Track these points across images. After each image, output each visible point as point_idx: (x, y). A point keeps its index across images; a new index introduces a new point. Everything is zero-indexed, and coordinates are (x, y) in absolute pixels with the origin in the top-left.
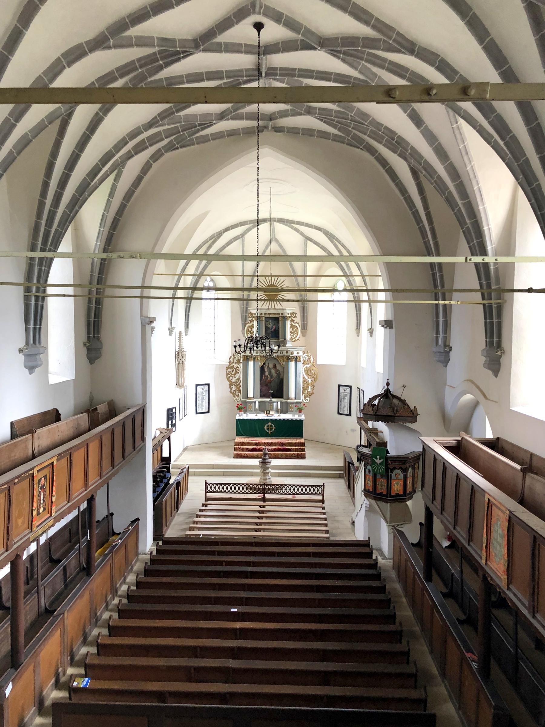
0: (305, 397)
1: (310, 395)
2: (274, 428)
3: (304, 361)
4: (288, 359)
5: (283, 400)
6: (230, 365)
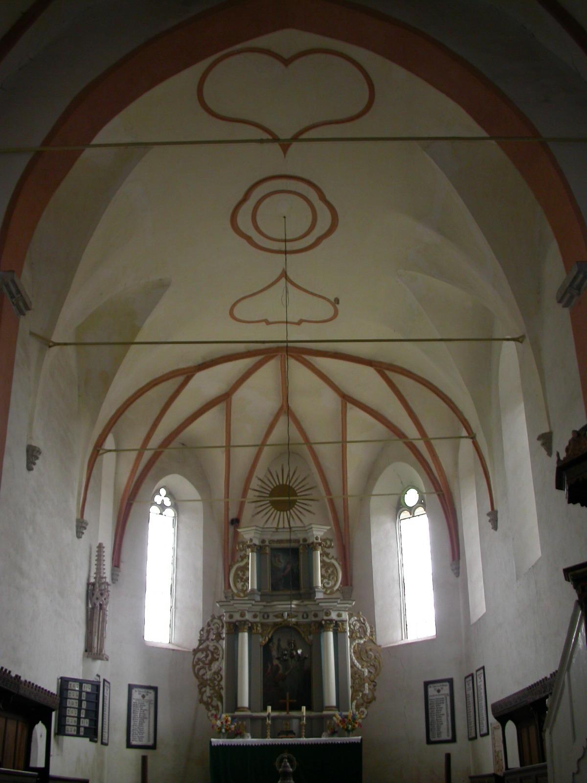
0: (357, 707)
1: (368, 702)
2: (295, 763)
3: (352, 632)
4: (321, 627)
5: (313, 714)
6: (200, 644)
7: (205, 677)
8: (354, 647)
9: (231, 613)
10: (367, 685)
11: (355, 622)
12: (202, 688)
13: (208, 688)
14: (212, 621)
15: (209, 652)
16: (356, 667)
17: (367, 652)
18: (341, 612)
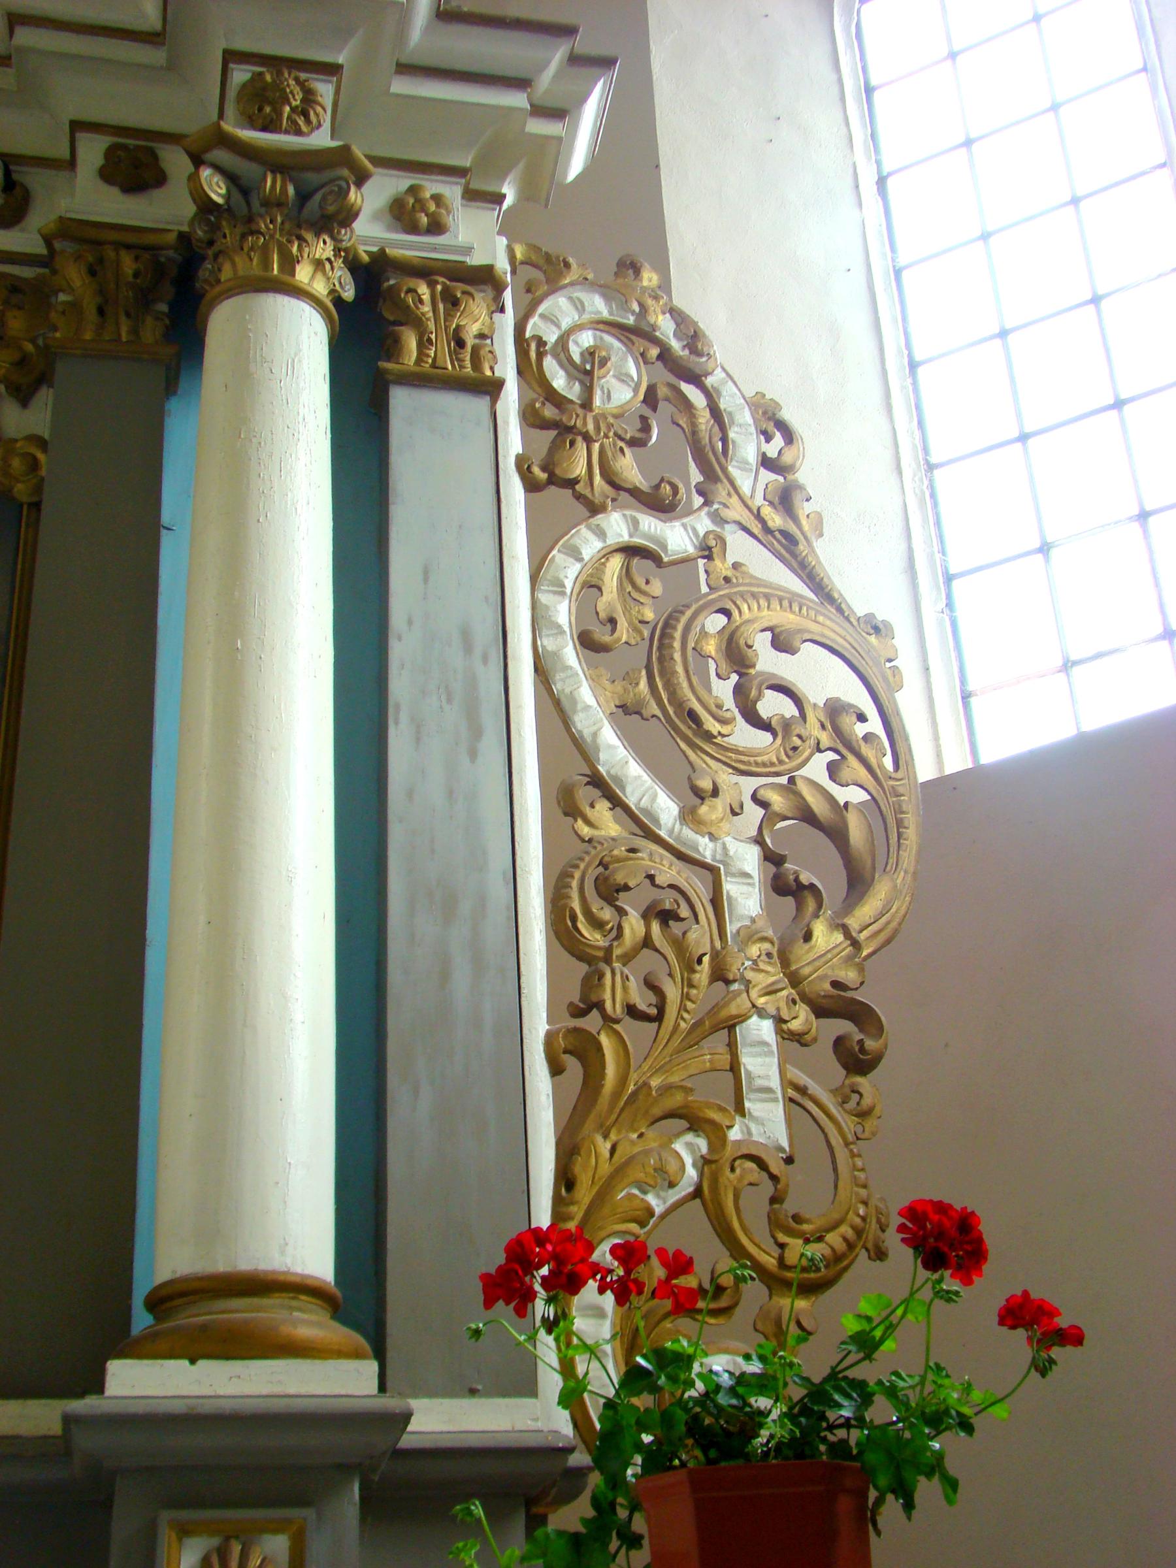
3: (554, 421)
8: (592, 585)
10: (762, 1029)
11: (586, 339)
16: (616, 802)
17: (737, 656)
18: (432, 186)
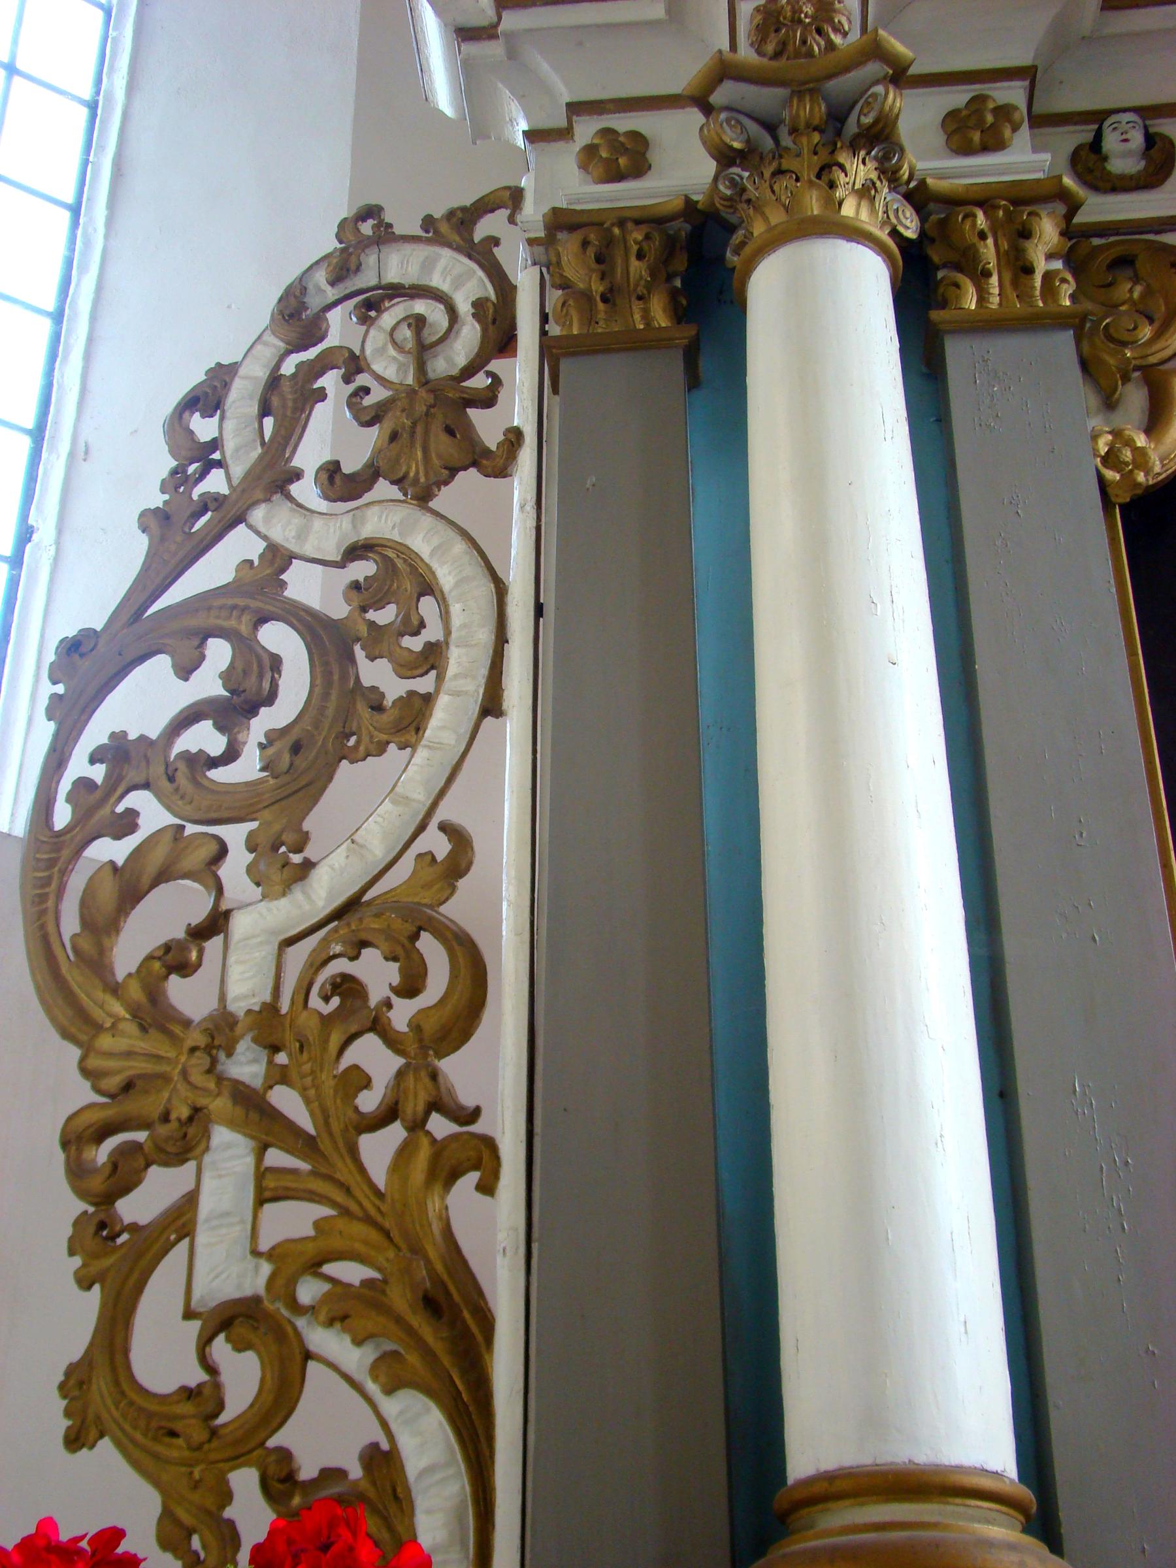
7: (189, 997)
9: (623, 123)
12: (124, 1176)
13: (229, 1155)
14: (342, 266)
15: (278, 638)
